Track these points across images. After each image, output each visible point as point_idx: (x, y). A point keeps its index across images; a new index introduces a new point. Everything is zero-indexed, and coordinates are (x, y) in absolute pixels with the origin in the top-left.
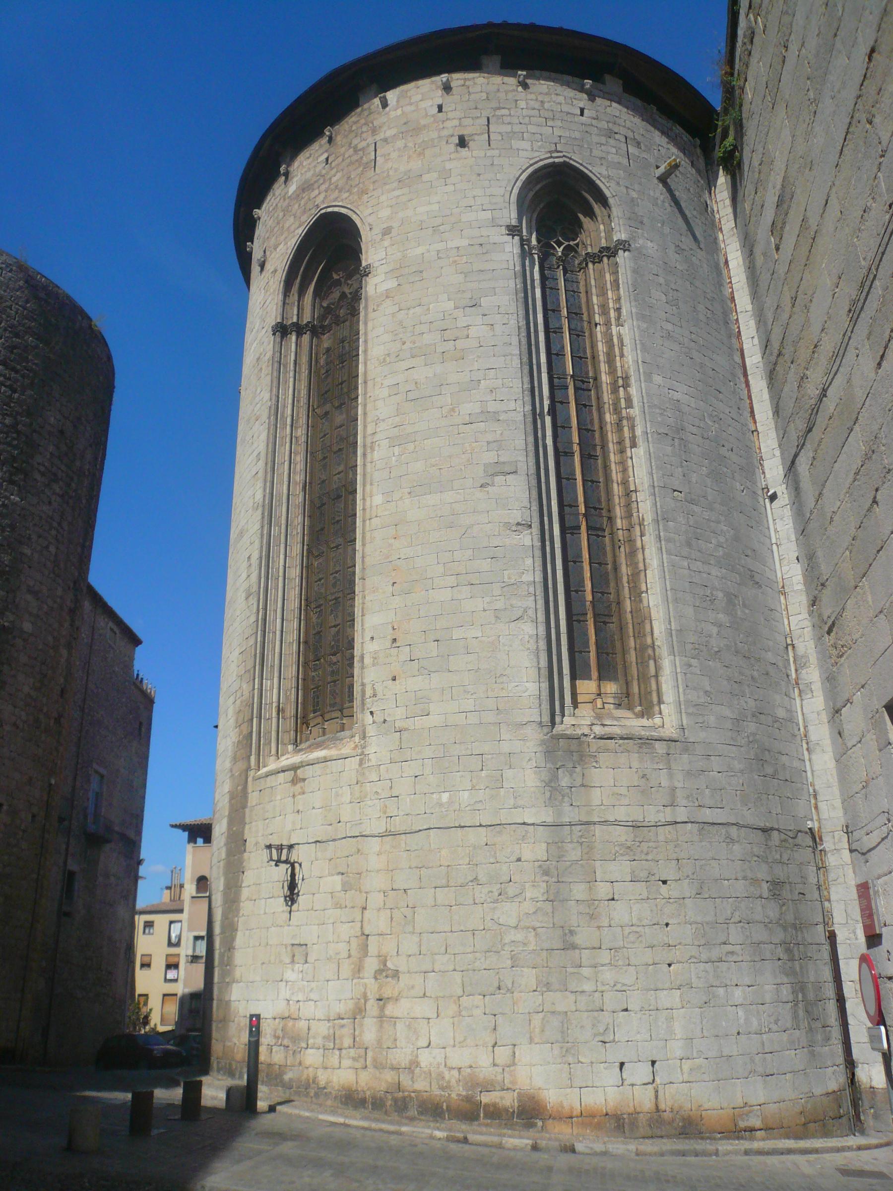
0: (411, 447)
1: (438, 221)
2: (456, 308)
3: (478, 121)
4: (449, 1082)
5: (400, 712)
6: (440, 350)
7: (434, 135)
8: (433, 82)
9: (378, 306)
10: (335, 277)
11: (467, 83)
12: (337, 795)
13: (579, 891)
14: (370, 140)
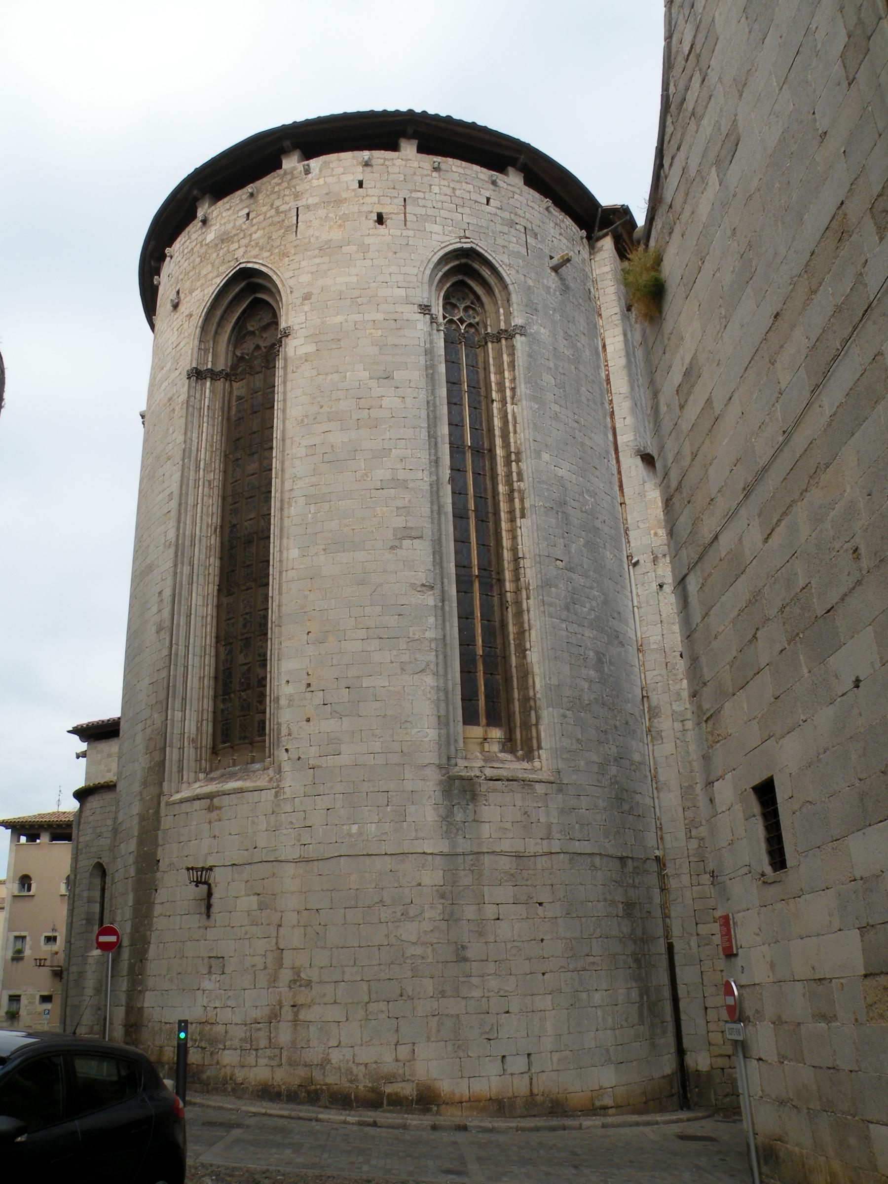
0: (326, 506)
1: (356, 293)
2: (371, 378)
3: (395, 201)
4: (357, 1075)
5: (314, 751)
6: (355, 417)
7: (356, 209)
8: (354, 158)
9: (297, 368)
10: (251, 329)
11: (387, 163)
12: (253, 823)
13: (470, 912)
14: (293, 205)
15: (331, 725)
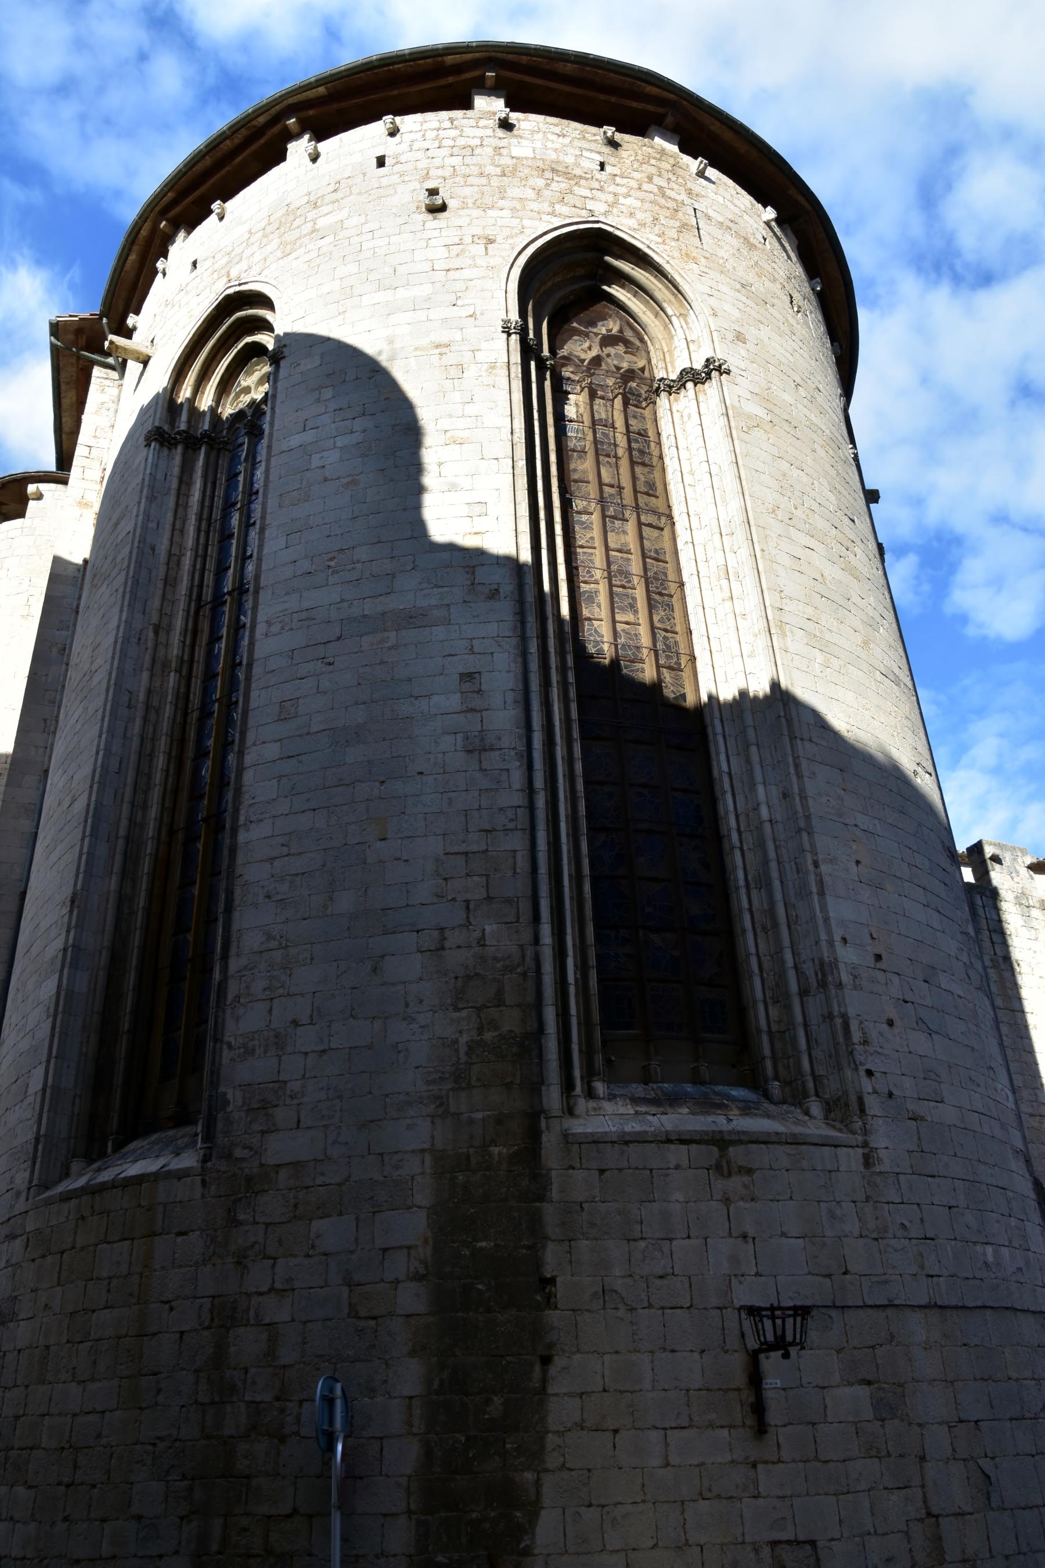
12: (832, 1216)
15: (920, 1043)
